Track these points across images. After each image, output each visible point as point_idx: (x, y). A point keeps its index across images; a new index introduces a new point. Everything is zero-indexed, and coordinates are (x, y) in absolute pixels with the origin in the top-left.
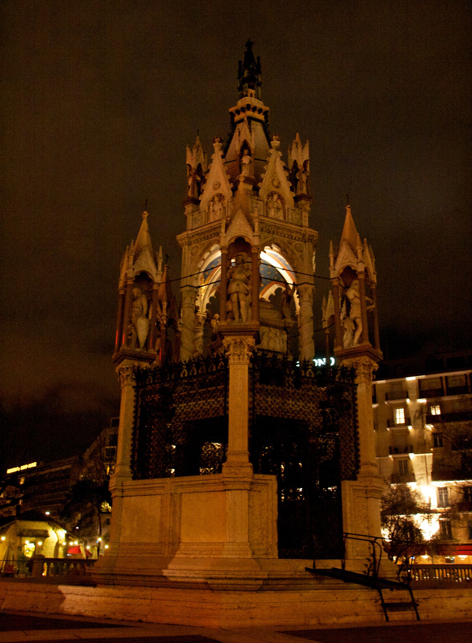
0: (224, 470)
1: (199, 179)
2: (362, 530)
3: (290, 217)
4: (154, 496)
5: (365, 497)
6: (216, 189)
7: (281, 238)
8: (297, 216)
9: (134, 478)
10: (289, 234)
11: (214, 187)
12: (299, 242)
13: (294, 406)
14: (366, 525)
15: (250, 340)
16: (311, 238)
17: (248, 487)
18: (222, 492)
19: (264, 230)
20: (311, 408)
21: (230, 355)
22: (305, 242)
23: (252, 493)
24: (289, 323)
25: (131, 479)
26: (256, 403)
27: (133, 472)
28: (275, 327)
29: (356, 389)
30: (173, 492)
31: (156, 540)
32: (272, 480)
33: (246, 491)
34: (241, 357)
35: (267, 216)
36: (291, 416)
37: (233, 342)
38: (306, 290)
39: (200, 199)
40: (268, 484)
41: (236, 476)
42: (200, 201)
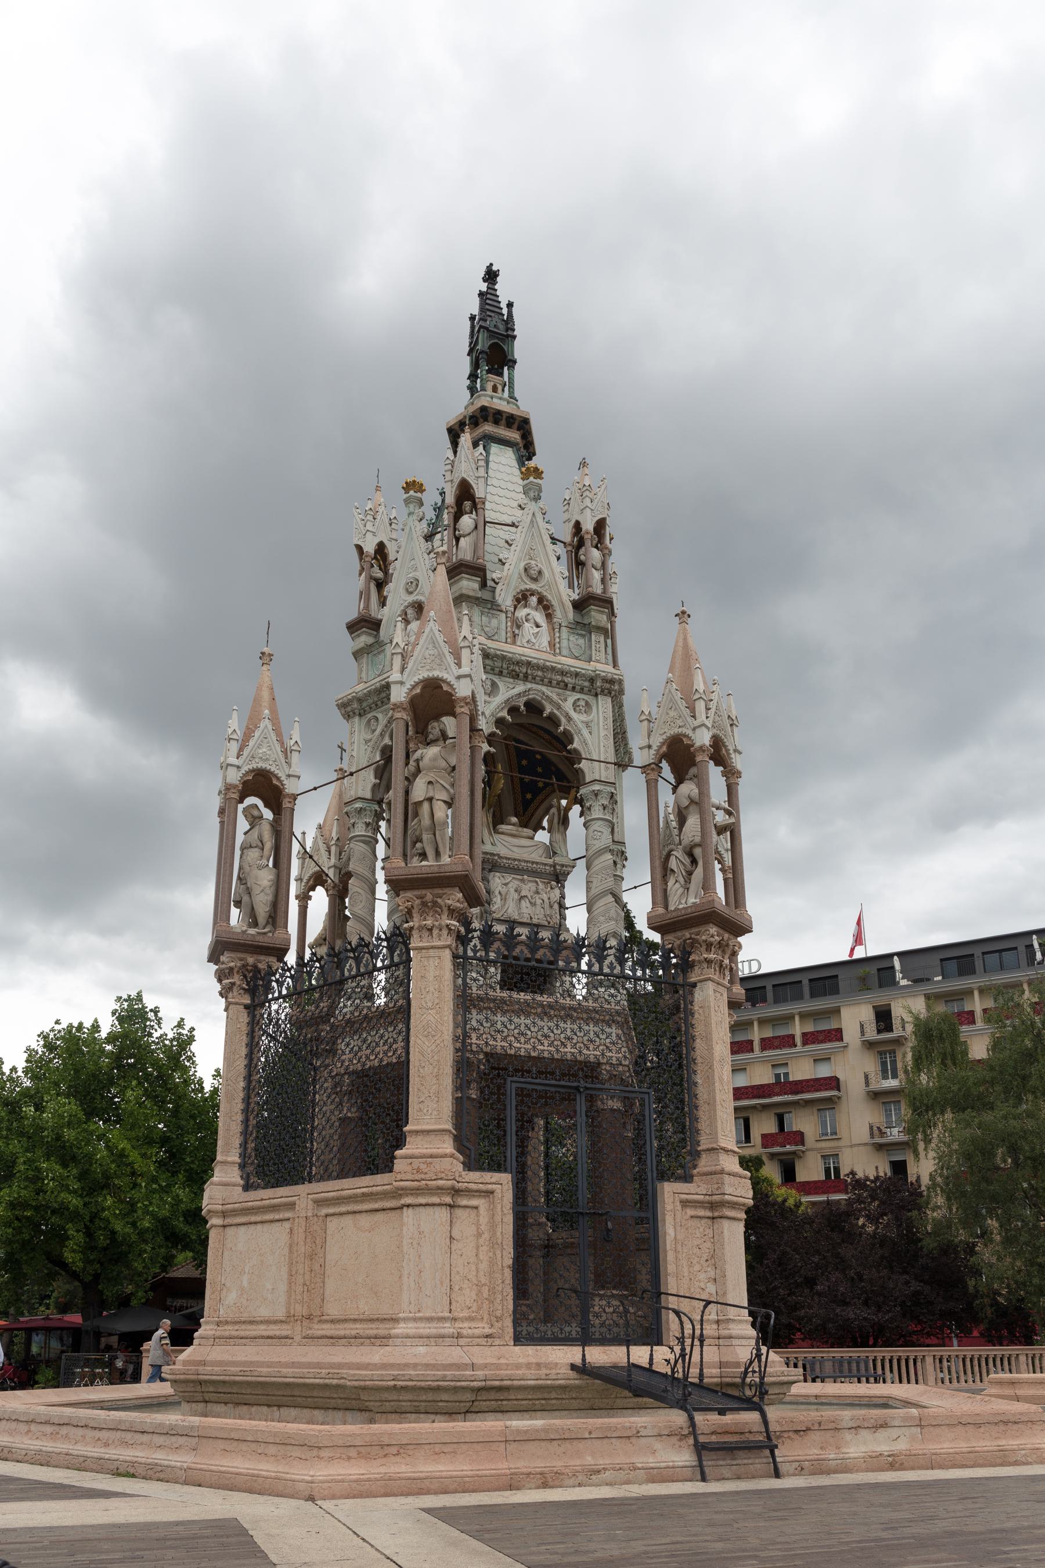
0: (399, 1165)
1: (380, 575)
2: (702, 1285)
3: (564, 643)
4: (278, 1224)
5: (709, 1218)
6: (411, 593)
7: (544, 689)
8: (581, 641)
9: (247, 1188)
10: (559, 678)
11: (407, 590)
12: (585, 697)
13: (482, 1025)
14: (712, 1274)
15: (455, 898)
16: (608, 686)
17: (448, 1200)
18: (398, 1211)
19: (505, 672)
20: (522, 1028)
21: (412, 928)
22: (596, 695)
23: (458, 1212)
24: (563, 866)
25: (241, 1188)
26: (468, 1026)
27: (246, 1177)
28: (534, 873)
29: (692, 994)
30: (310, 1214)
31: (280, 1313)
32: (502, 1183)
33: (444, 1208)
34: (435, 932)
35: (514, 643)
36: (523, 1050)
37: (418, 902)
38: (596, 795)
39: (379, 617)
40: (492, 1192)
41: (423, 1176)
42: (381, 621)
